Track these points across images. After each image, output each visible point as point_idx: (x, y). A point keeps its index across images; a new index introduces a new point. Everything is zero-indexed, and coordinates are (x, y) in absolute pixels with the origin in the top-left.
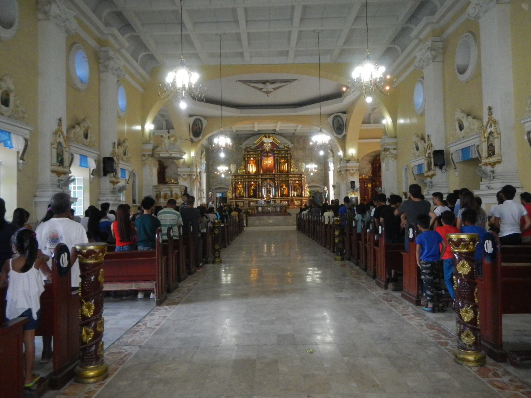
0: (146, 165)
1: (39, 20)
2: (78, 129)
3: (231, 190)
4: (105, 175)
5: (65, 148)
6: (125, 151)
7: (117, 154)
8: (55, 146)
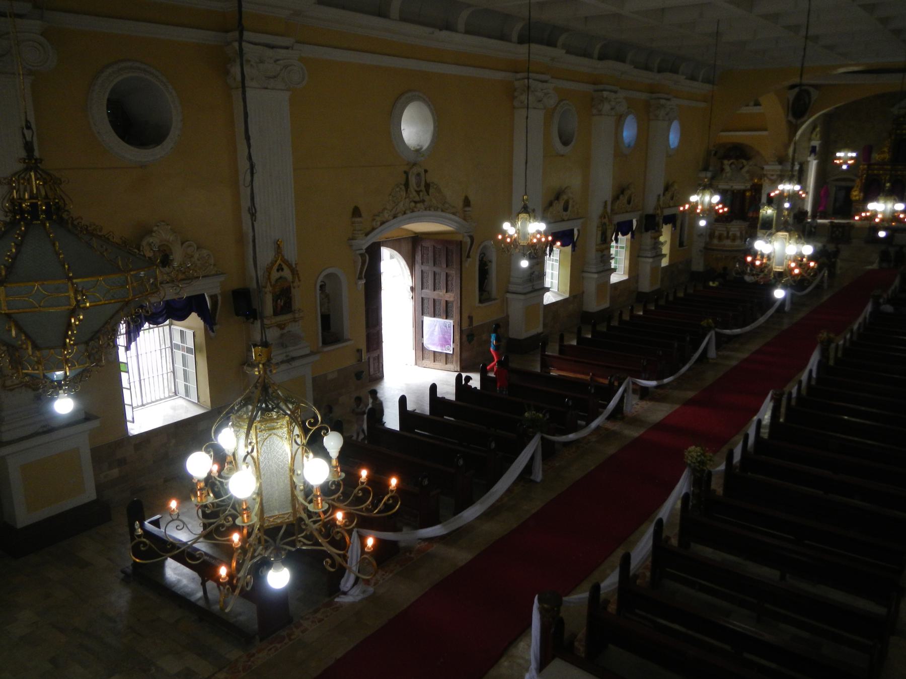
2: (621, 197)
3: (859, 186)
4: (647, 230)
5: (609, 226)
8: (601, 229)
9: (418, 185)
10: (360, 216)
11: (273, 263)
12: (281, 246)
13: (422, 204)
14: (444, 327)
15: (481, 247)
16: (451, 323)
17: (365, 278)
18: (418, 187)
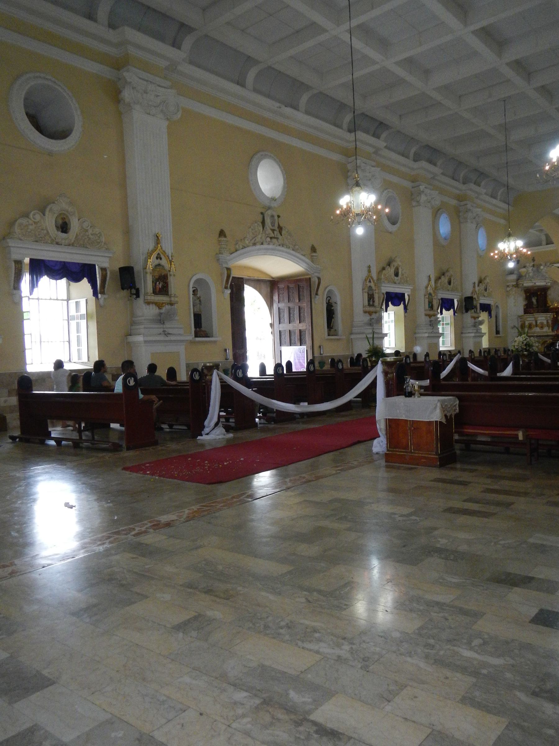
0: (510, 296)
1: (413, 207)
2: (443, 278)
4: (467, 311)
6: (485, 288)
7: (477, 292)
8: (427, 296)
9: (273, 224)
10: (225, 236)
11: (153, 251)
12: (159, 238)
13: (275, 240)
14: (299, 353)
15: (327, 290)
16: (304, 348)
17: (230, 288)
18: (273, 226)
